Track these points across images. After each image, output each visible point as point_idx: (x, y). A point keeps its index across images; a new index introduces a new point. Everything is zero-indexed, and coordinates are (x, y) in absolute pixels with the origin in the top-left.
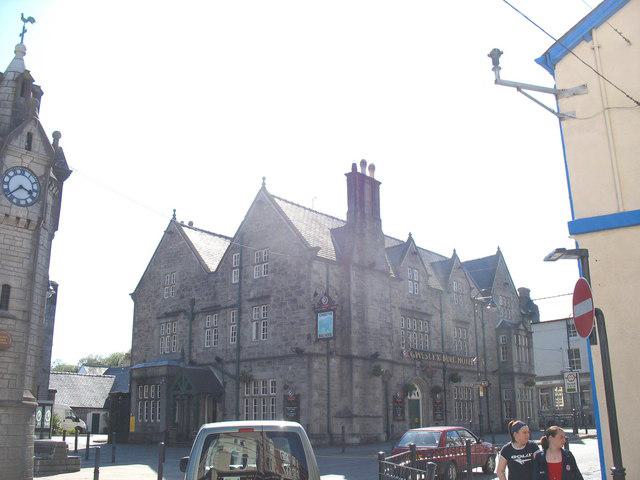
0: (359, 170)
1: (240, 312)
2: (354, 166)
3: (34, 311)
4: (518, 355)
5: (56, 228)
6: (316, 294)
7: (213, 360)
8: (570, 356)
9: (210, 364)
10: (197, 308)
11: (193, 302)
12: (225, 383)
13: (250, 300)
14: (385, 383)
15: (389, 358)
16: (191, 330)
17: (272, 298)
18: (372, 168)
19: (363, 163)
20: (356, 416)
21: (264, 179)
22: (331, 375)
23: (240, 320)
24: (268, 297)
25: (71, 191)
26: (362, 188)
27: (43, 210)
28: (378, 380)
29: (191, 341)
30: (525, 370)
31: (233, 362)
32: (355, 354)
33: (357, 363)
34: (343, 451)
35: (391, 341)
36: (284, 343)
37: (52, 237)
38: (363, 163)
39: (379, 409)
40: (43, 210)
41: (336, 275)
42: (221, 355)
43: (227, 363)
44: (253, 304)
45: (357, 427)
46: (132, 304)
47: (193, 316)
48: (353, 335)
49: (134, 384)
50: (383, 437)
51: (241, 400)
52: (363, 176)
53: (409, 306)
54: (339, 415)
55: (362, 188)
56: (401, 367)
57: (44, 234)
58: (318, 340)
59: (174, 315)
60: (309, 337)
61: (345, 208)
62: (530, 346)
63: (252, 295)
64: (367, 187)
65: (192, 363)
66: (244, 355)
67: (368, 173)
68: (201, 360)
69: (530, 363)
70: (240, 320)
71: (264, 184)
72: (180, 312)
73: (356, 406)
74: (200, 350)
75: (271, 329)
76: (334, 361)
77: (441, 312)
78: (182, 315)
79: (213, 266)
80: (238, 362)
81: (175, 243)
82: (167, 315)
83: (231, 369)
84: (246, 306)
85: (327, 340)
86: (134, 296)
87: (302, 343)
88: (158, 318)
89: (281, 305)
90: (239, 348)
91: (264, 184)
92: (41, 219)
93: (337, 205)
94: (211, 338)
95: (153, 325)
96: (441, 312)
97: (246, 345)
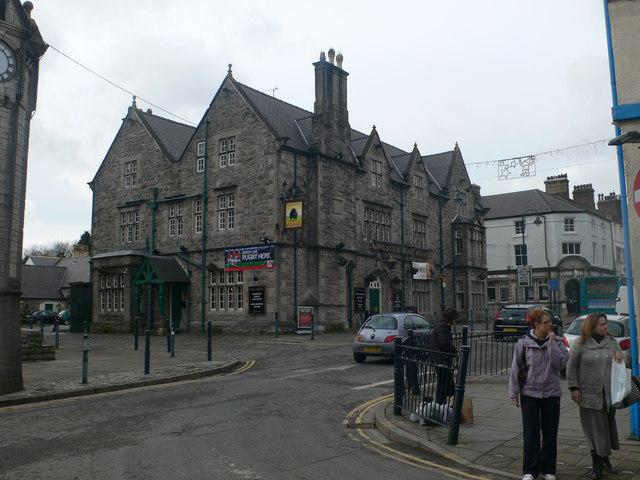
0: (328, 60)
1: (206, 202)
2: (323, 54)
3: (15, 195)
4: (471, 251)
5: (33, 107)
6: (285, 184)
7: (179, 250)
8: (517, 252)
9: (176, 254)
10: (161, 198)
11: (156, 192)
12: (190, 272)
13: (216, 190)
14: (349, 273)
15: (353, 248)
16: (154, 220)
17: (239, 188)
18: (340, 59)
19: (331, 52)
20: (322, 305)
21: (230, 66)
22: (298, 264)
23: (206, 209)
24: (235, 187)
25: (49, 71)
26: (330, 76)
27: (20, 86)
28: (343, 269)
29: (155, 231)
30: (478, 264)
31: (199, 252)
32: (322, 244)
33: (324, 253)
34: (313, 339)
35: (355, 232)
36: (251, 233)
37: (29, 117)
38: (331, 52)
39: (343, 298)
40: (20, 86)
41: (304, 166)
42: (186, 244)
43: (194, 252)
44: (221, 193)
45: (322, 315)
46: (90, 193)
47: (156, 208)
48: (319, 225)
49: (97, 273)
50: (347, 326)
51: (207, 291)
52: (331, 66)
53: (372, 199)
54: (307, 303)
55: (330, 76)
56: (362, 259)
57: (22, 113)
58: (286, 230)
59: (137, 204)
60: (277, 227)
61: (312, 99)
62: (482, 242)
63: (218, 184)
64: (335, 78)
65: (156, 252)
66: (210, 245)
67: (335, 64)
68: (165, 250)
69: (483, 259)
70: (206, 209)
71: (230, 71)
72: (143, 201)
73: (322, 294)
74: (164, 240)
75: (237, 218)
76: (300, 251)
77: (402, 206)
78: (143, 207)
79: (311, 109)
80: (204, 252)
81: (139, 126)
82: (129, 205)
83: (197, 260)
84: (213, 195)
85: (294, 230)
86: (92, 185)
87: (271, 233)
88: (119, 208)
89: (249, 195)
90: (205, 238)
91: (230, 71)
92: (19, 97)
93: (303, 96)
94: (177, 231)
95: (112, 214)
96: (402, 206)
97: (212, 234)
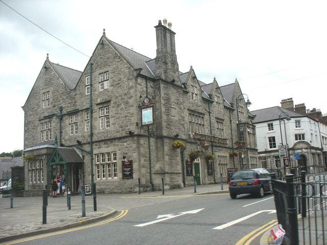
1: (92, 112)
2: (160, 21)
4: (249, 139)
6: (141, 97)
8: (270, 141)
9: (74, 146)
10: (64, 112)
11: (61, 109)
12: (83, 157)
13: (98, 104)
14: (182, 153)
15: (184, 137)
16: (61, 126)
17: (112, 102)
19: (165, 21)
20: (167, 173)
23: (92, 117)
24: (109, 101)
26: (164, 32)
28: (179, 150)
29: (61, 132)
30: (253, 147)
31: (89, 143)
33: (166, 140)
34: (163, 194)
36: (121, 129)
39: (179, 168)
42: (80, 139)
43: (85, 144)
44: (100, 106)
45: (167, 179)
46: (23, 113)
47: (61, 118)
50: (183, 185)
51: (94, 167)
53: (193, 109)
55: (164, 32)
56: (189, 144)
58: (142, 126)
59: (50, 117)
60: (137, 124)
62: (254, 134)
63: (99, 101)
64: (168, 35)
65: (62, 145)
66: (95, 138)
69: (255, 144)
70: (92, 117)
74: (67, 137)
75: (111, 120)
77: (210, 113)
78: (55, 117)
82: (45, 118)
84: (96, 108)
85: (148, 126)
87: (133, 128)
88: (40, 120)
89: (118, 106)
90: (92, 135)
93: (148, 49)
95: (36, 124)
96: (210, 113)
97: (95, 132)
